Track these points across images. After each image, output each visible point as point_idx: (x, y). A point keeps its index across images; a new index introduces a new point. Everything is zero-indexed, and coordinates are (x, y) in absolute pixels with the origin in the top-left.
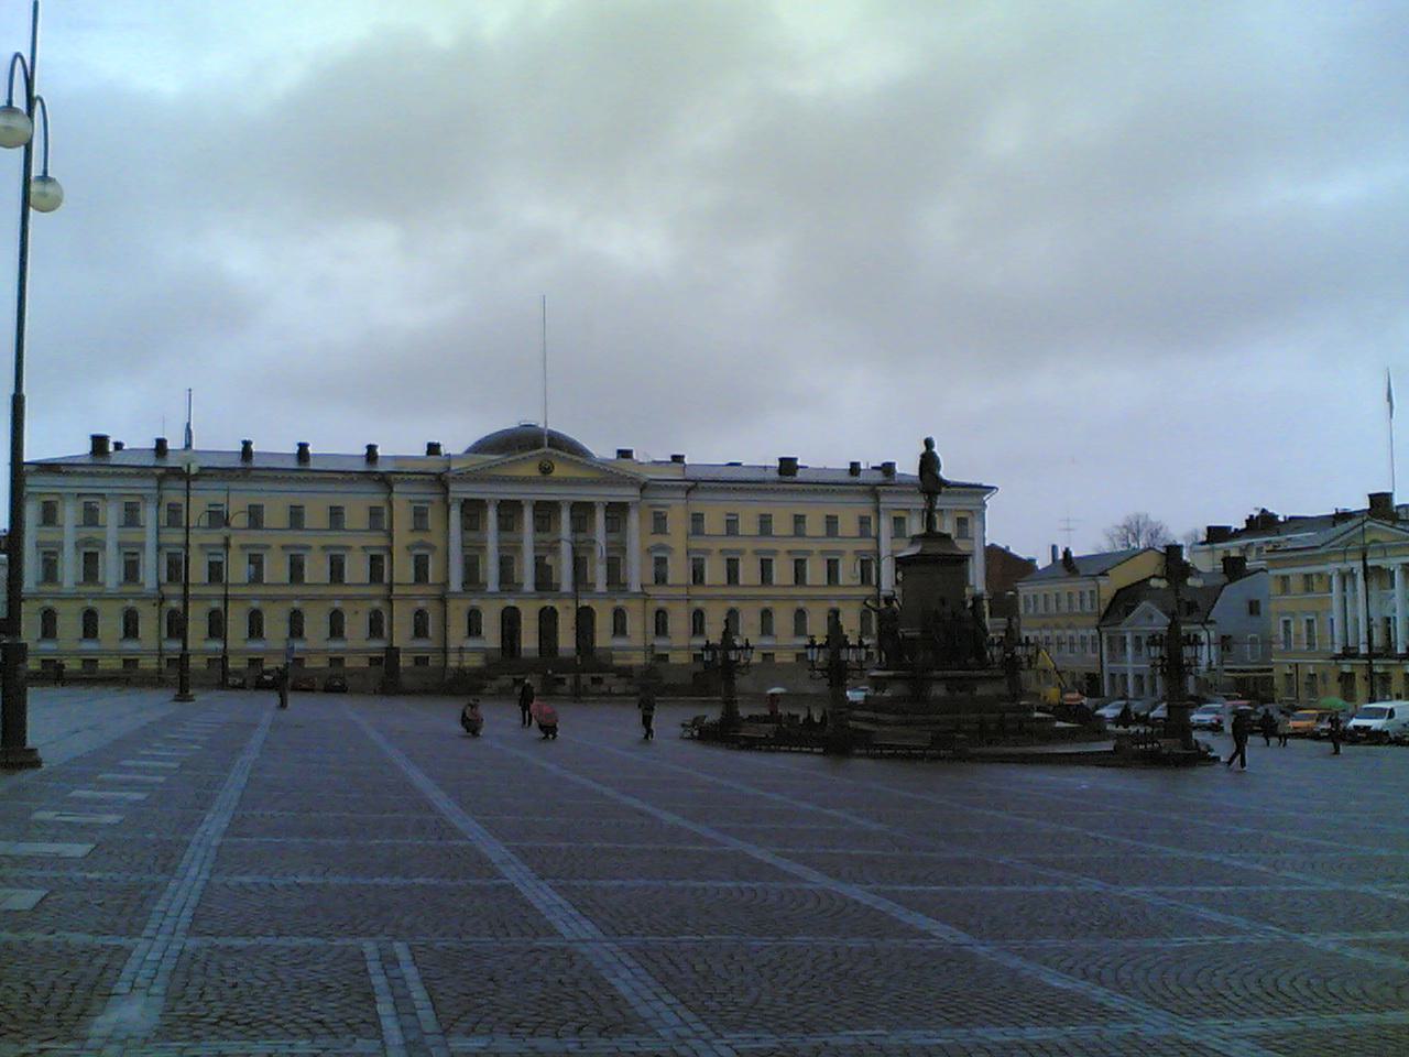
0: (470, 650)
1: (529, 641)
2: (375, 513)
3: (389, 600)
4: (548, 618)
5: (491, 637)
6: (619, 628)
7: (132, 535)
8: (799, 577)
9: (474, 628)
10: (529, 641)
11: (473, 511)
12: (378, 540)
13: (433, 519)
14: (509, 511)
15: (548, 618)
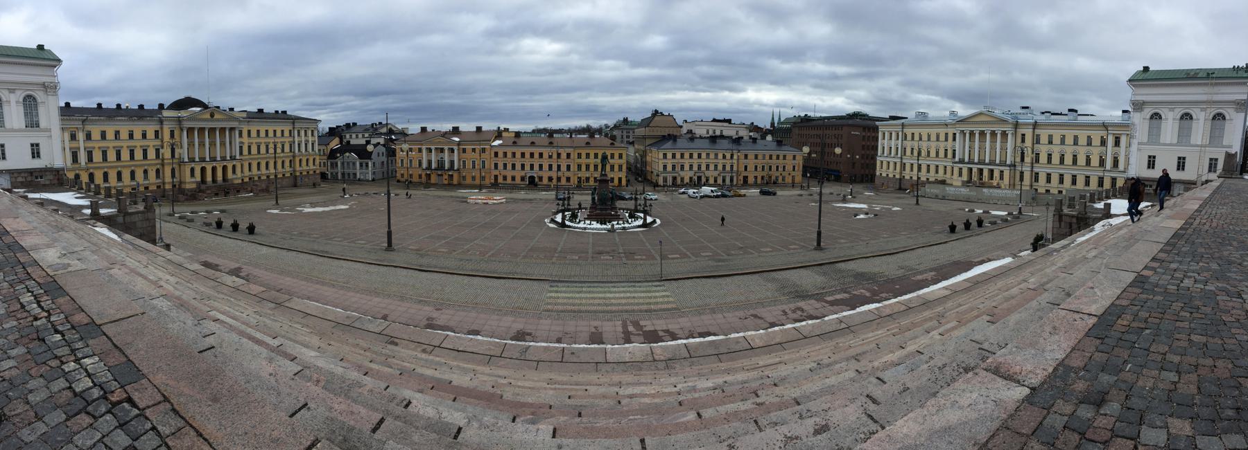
0: (190, 183)
1: (209, 178)
2: (157, 132)
3: (163, 165)
4: (214, 169)
5: (198, 178)
6: (234, 172)
7: (74, 144)
8: (119, 158)
9: (192, 174)
10: (209, 178)
11: (190, 130)
12: (158, 143)
13: (176, 133)
14: (201, 130)
15: (214, 169)
